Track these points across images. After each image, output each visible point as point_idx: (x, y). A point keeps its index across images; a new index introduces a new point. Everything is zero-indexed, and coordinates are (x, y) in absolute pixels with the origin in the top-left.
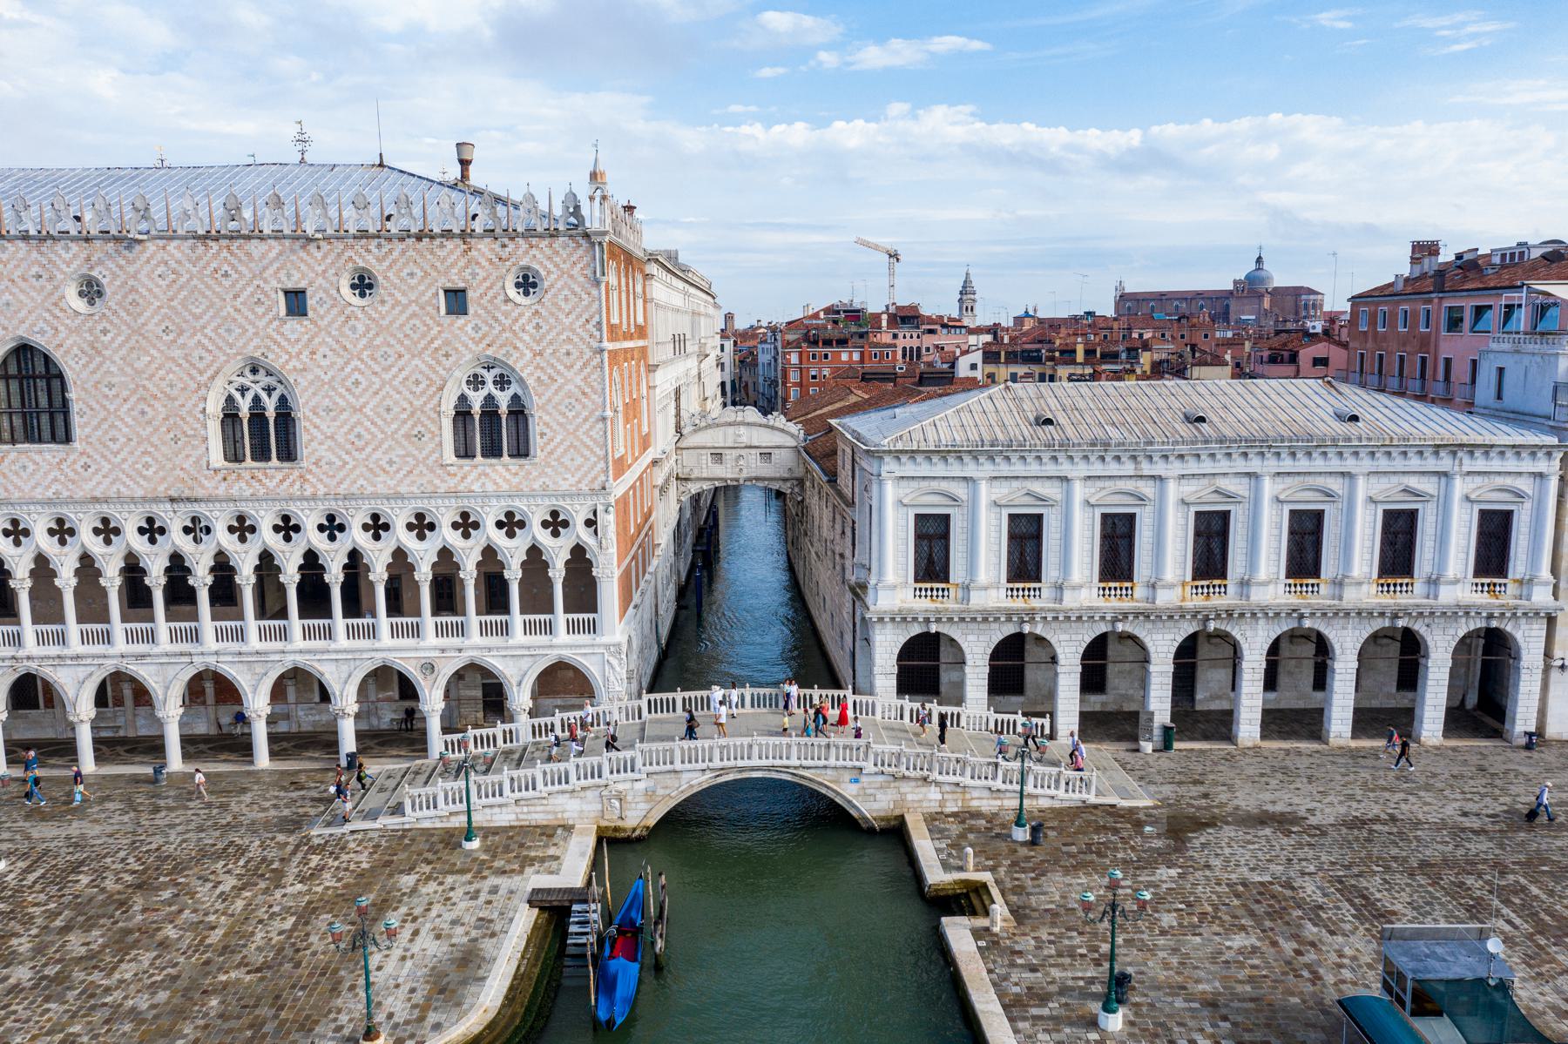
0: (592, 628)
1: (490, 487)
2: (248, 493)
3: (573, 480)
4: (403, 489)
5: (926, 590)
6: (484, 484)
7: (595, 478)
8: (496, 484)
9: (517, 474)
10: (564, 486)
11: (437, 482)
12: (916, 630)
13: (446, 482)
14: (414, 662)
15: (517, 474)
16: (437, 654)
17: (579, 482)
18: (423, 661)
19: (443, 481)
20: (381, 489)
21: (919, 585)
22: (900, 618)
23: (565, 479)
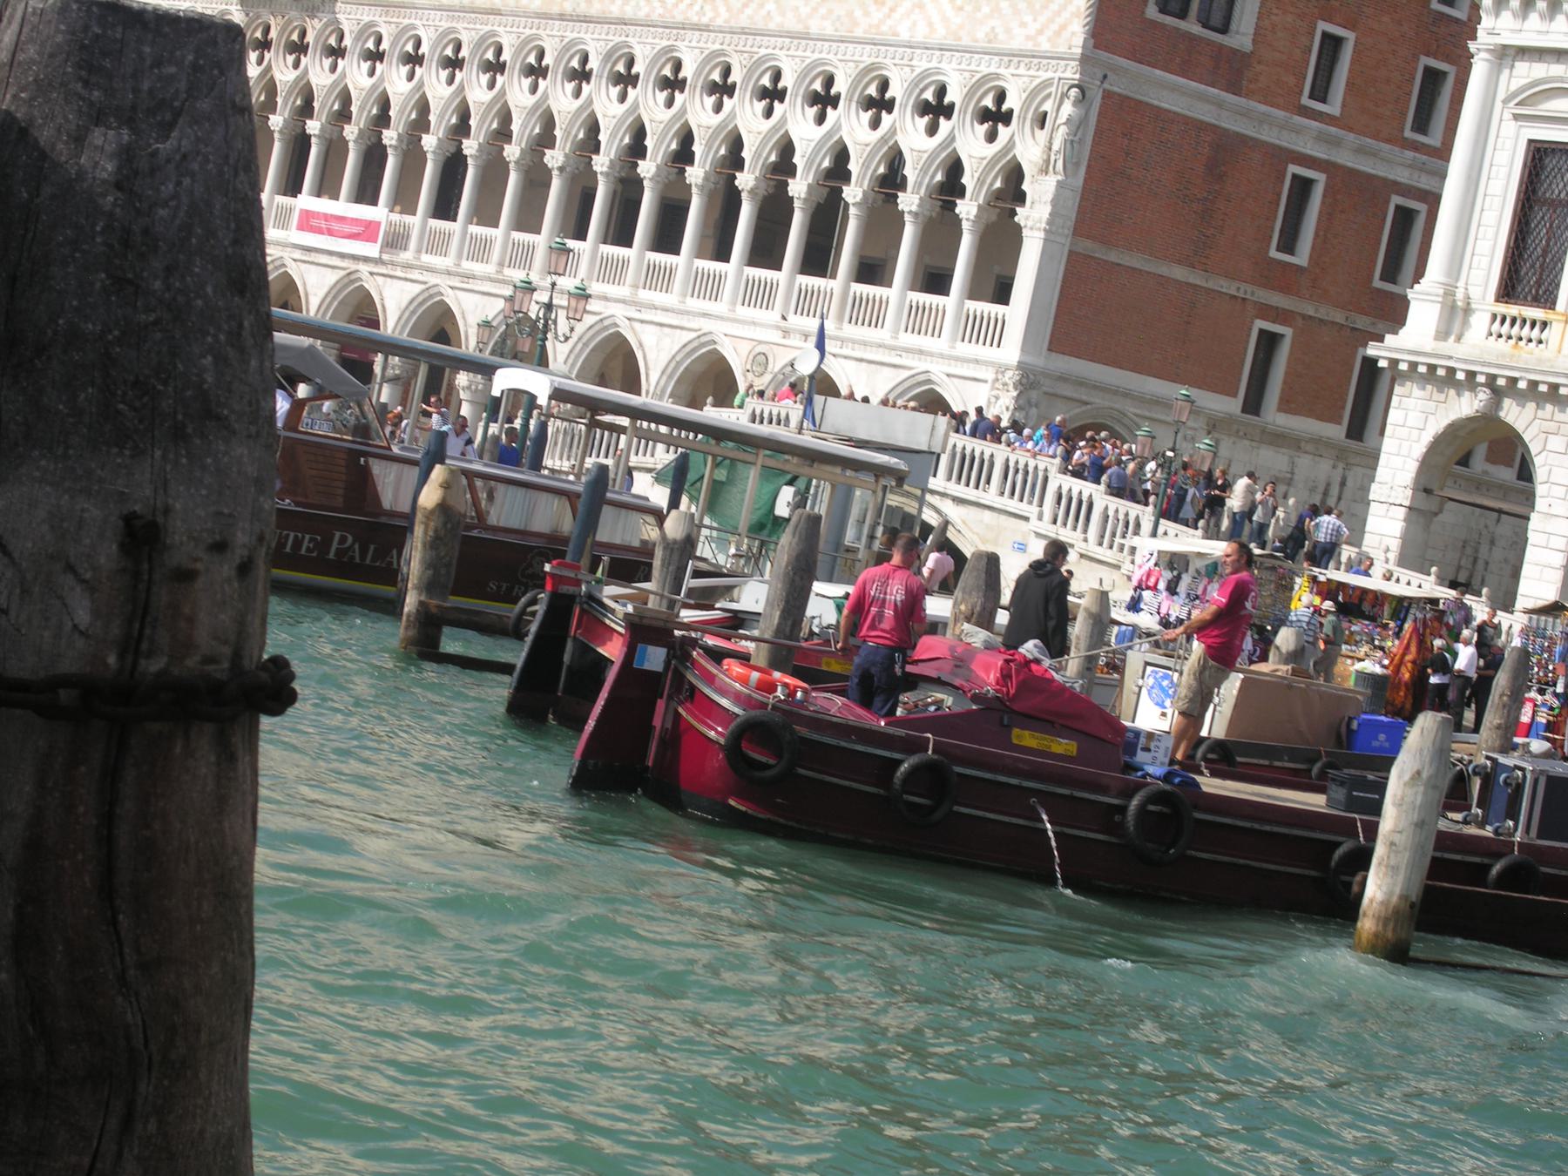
0: (992, 333)
1: (920, 35)
2: (641, 14)
3: (1033, 28)
4: (815, 27)
5: (1514, 321)
6: (914, 24)
7: (1063, 27)
8: (930, 25)
9: (961, 9)
10: (1018, 42)
11: (858, 13)
12: (1467, 405)
13: (867, 14)
14: (745, 348)
15: (961, 9)
16: (775, 336)
17: (1040, 32)
18: (760, 349)
19: (867, 14)
20: (791, 24)
21: (1503, 309)
22: (1443, 379)
23: (1023, 25)
